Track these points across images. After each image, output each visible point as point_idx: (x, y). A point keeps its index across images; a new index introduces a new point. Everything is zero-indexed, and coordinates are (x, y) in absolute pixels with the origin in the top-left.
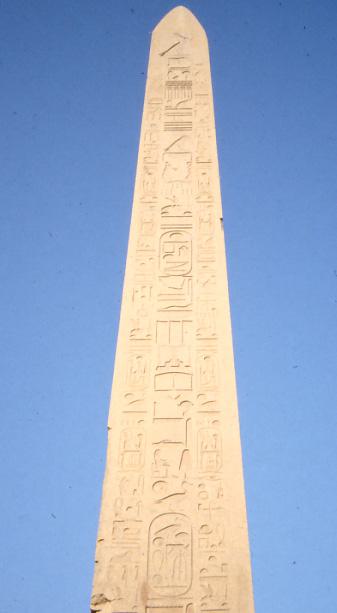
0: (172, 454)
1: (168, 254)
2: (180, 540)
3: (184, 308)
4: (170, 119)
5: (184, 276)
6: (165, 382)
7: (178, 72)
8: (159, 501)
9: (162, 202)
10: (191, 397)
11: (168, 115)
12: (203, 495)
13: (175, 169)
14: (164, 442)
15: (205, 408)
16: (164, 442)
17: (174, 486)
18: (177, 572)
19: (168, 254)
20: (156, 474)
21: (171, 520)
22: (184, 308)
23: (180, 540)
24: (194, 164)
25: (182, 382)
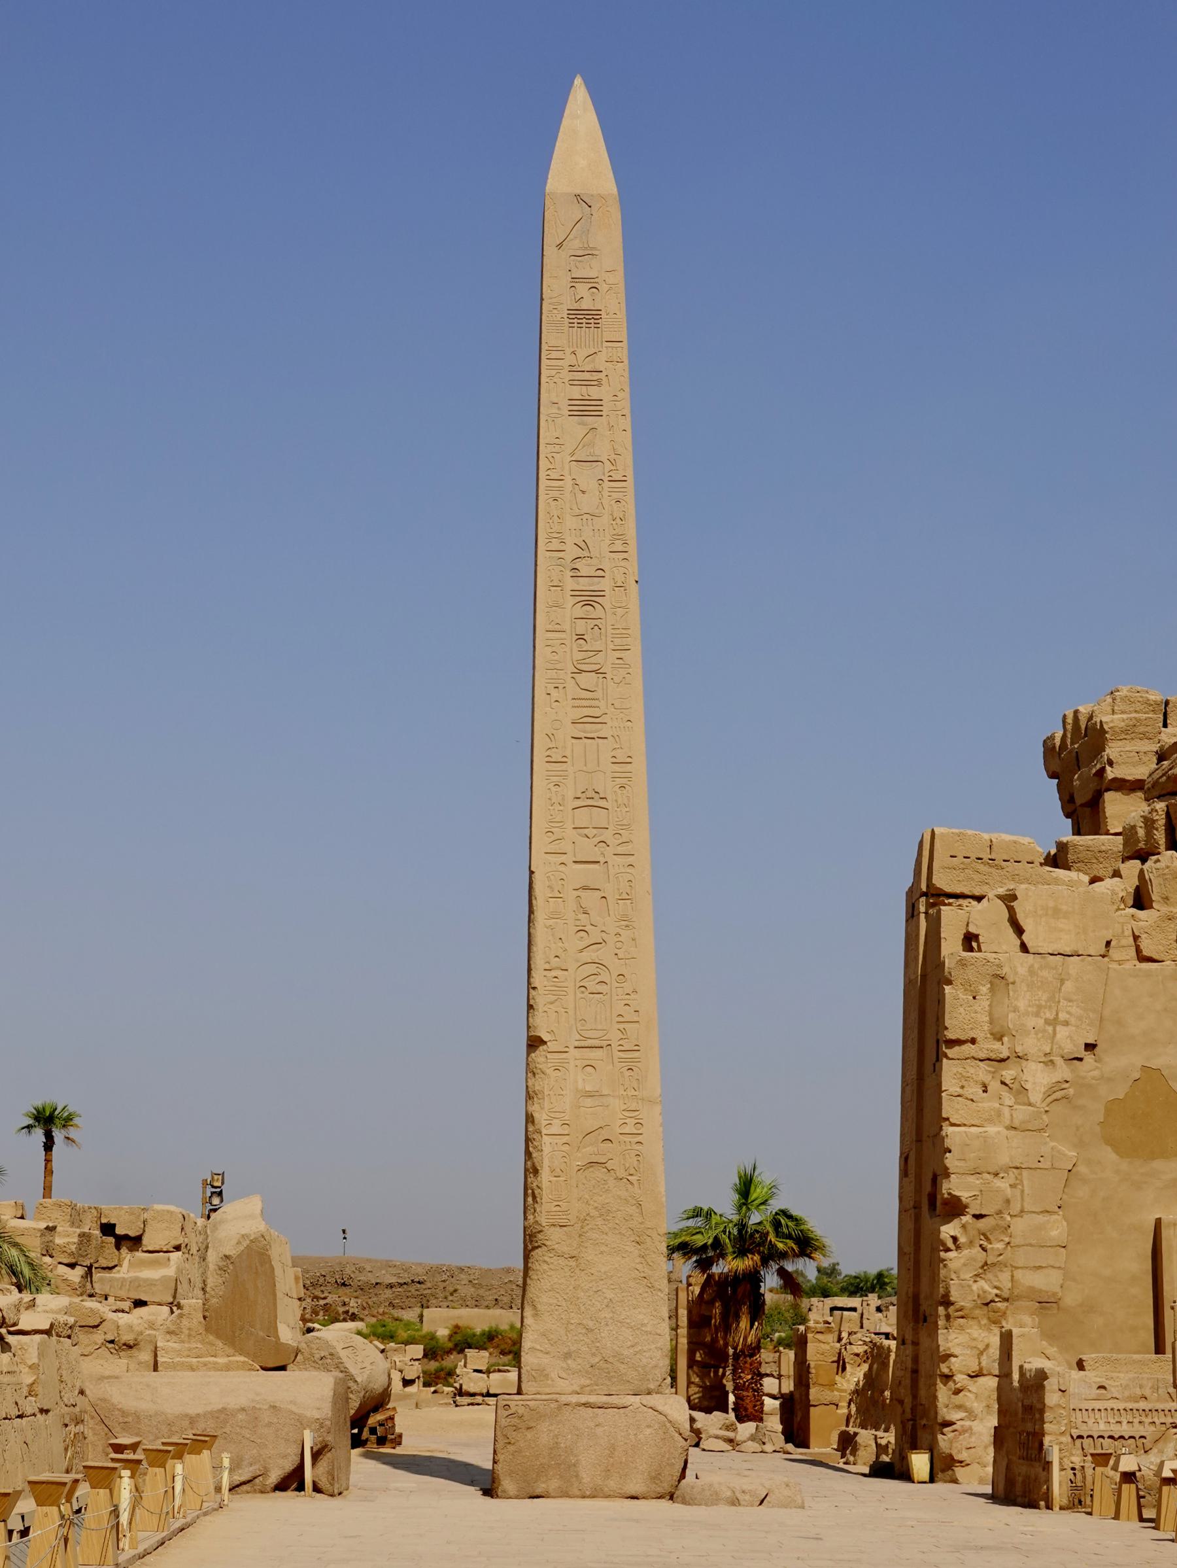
0: (591, 899)
1: (581, 637)
2: (600, 988)
3: (595, 720)
4: (576, 392)
5: (596, 672)
6: (583, 817)
7: (582, 289)
8: (581, 951)
9: (571, 552)
10: (607, 835)
11: (572, 383)
12: (619, 945)
13: (583, 492)
14: (585, 888)
15: (620, 850)
16: (585, 888)
17: (596, 936)
18: (598, 1017)
19: (581, 637)
20: (578, 923)
21: (592, 969)
22: (595, 720)
23: (600, 988)
24: (607, 484)
25: (600, 817)
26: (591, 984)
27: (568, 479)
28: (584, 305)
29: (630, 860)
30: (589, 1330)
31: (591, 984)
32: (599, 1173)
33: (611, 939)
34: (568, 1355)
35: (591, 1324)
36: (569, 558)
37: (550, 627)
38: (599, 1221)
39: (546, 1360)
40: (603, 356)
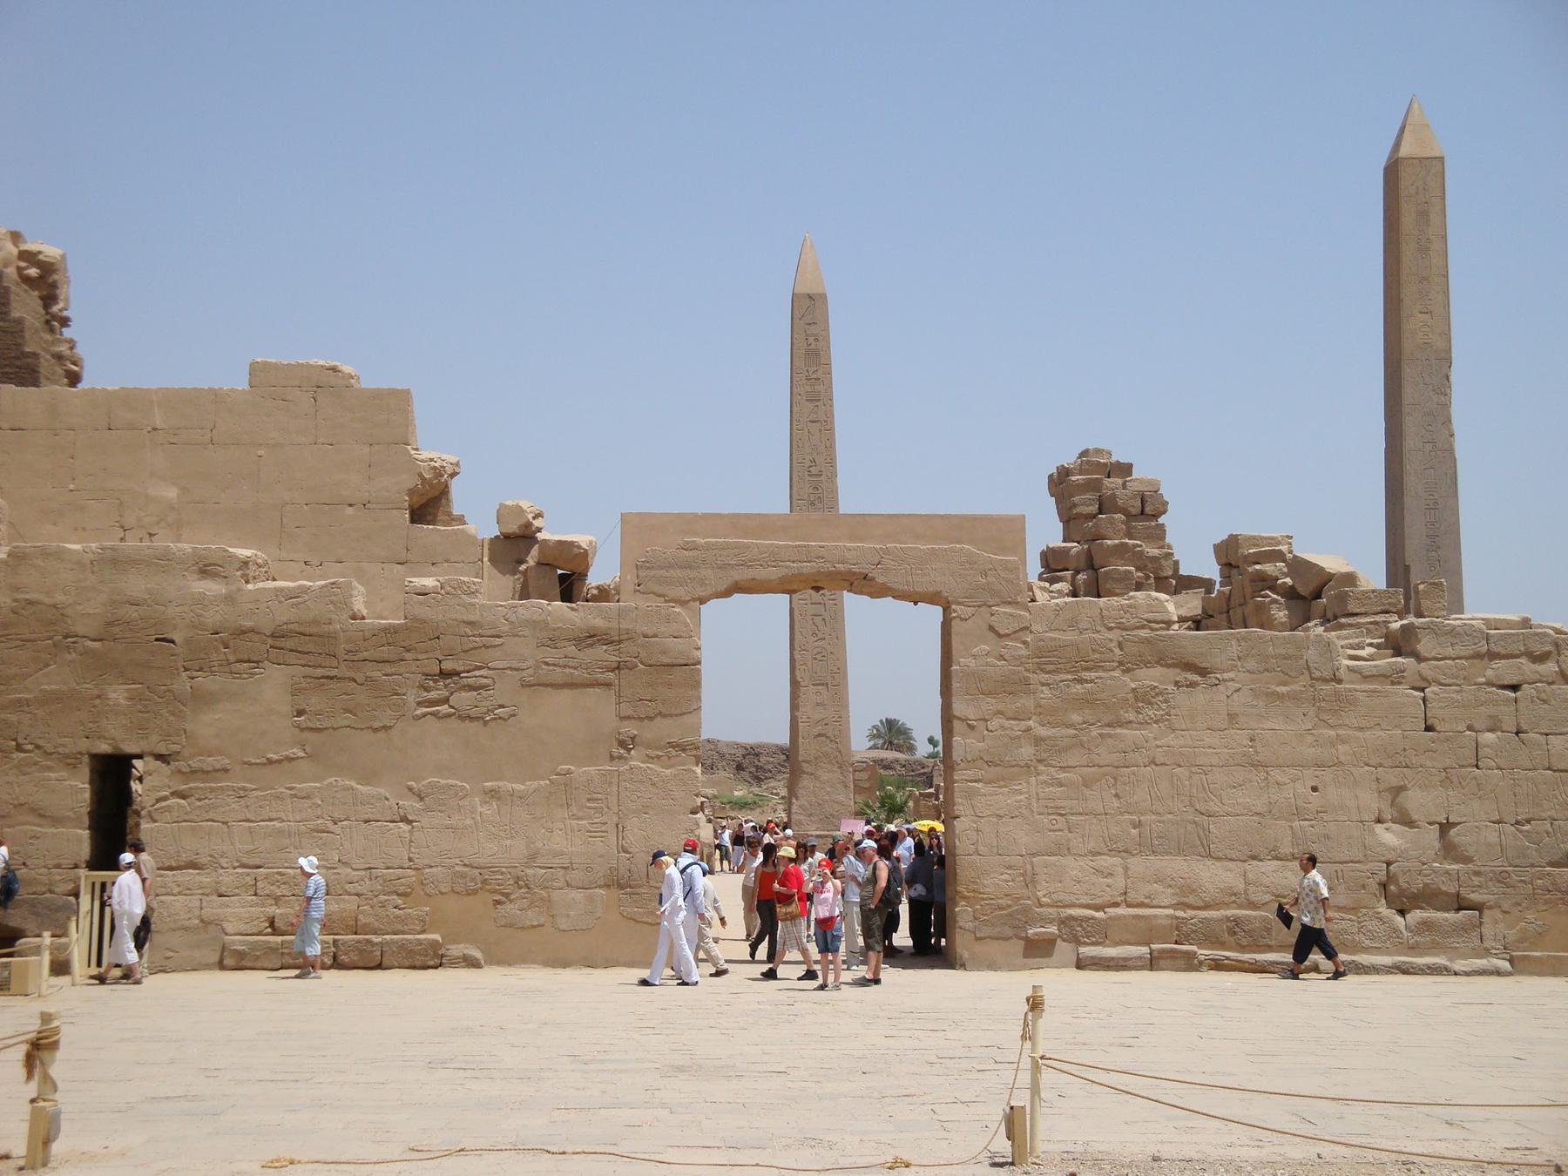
0: (818, 620)
4: (808, 388)
26: (818, 656)
27: (806, 429)
28: (813, 346)
29: (833, 602)
30: (820, 804)
31: (818, 656)
32: (824, 738)
33: (827, 637)
34: (810, 815)
35: (821, 802)
36: (806, 466)
37: (799, 498)
38: (824, 759)
39: (802, 817)
40: (820, 372)
